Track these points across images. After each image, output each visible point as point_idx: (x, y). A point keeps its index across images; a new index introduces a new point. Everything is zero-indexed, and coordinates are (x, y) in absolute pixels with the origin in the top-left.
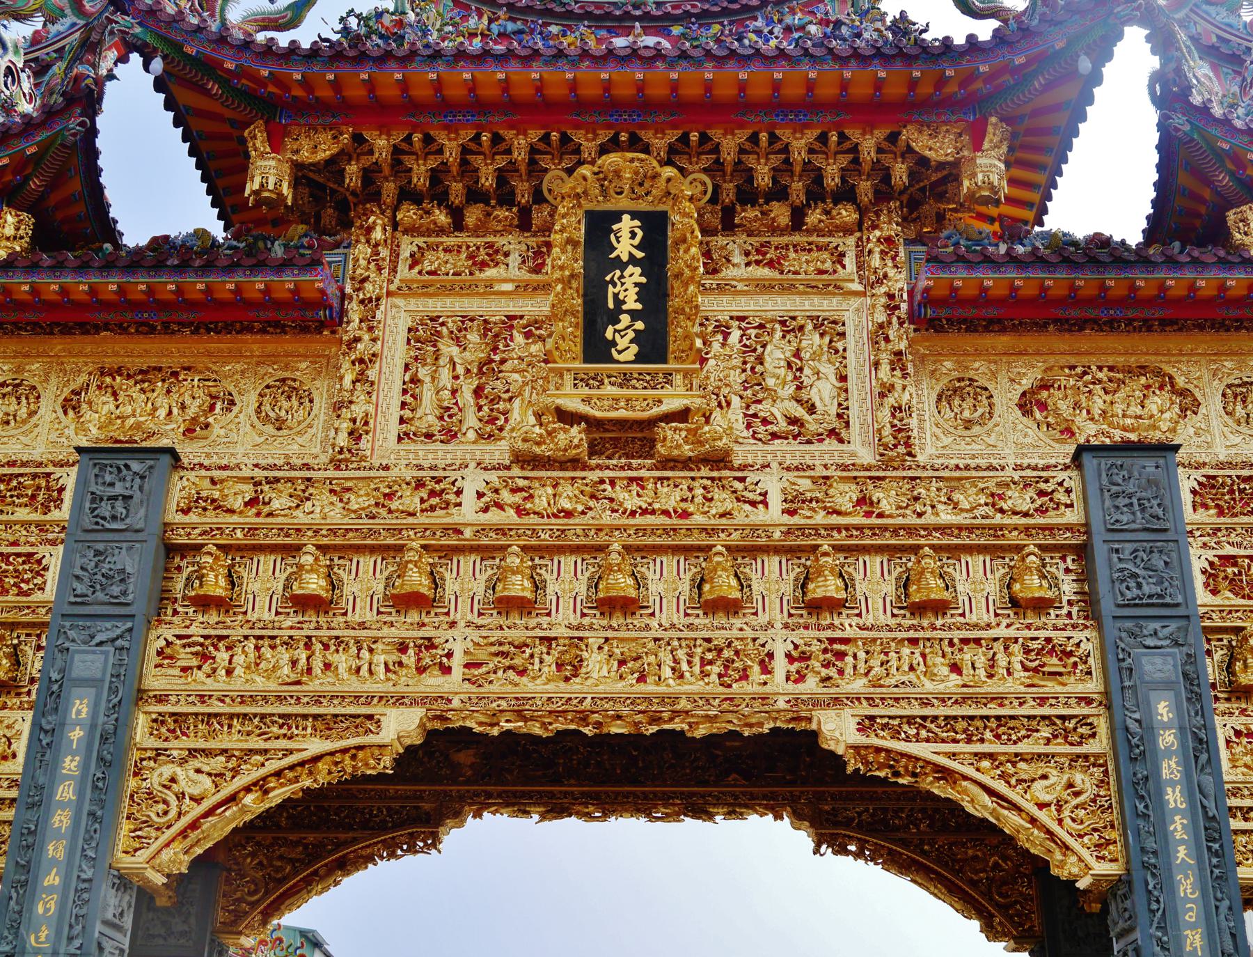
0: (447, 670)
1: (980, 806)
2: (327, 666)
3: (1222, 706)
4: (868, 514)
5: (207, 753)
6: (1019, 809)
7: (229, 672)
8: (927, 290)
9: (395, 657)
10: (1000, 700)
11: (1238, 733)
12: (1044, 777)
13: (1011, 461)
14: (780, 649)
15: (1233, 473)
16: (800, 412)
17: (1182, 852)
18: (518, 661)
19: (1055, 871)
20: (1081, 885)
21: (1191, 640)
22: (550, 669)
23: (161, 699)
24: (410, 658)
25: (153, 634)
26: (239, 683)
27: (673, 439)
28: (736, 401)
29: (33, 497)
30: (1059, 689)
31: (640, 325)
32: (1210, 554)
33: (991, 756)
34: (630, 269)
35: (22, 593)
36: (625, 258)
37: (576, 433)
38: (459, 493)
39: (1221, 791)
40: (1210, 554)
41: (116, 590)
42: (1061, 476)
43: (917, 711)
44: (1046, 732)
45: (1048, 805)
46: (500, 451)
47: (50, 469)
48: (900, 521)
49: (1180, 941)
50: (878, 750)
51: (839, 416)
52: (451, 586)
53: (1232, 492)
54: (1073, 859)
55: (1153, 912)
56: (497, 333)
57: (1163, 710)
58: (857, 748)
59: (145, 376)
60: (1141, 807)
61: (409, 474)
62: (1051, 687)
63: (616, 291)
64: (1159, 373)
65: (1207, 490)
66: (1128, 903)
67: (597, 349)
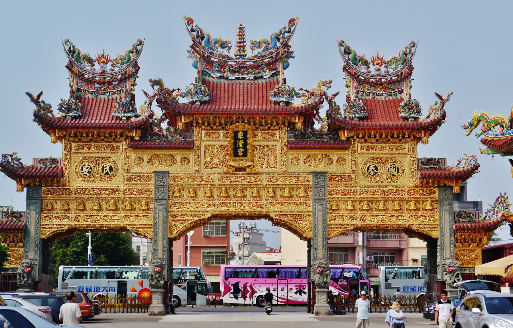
31: (243, 150)
67: (236, 154)
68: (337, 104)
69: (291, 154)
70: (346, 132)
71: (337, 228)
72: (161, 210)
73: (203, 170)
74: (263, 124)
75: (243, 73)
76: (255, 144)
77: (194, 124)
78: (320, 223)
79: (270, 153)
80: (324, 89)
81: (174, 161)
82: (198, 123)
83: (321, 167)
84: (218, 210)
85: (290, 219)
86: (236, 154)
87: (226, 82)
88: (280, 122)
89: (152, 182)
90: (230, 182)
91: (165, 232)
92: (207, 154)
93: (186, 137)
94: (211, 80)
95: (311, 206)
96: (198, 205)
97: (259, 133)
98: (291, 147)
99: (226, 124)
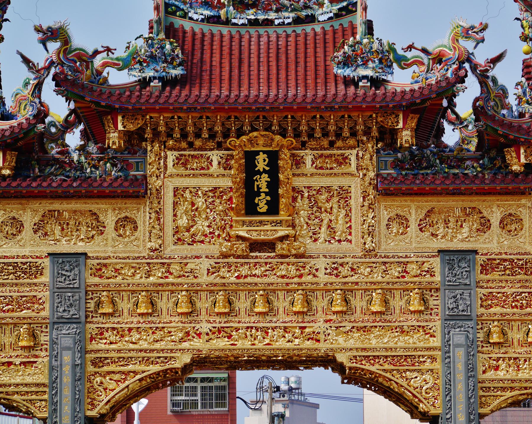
31: (268, 198)
34: (264, 175)
36: (261, 170)
63: (258, 184)
67: (251, 209)
68: (500, 81)
69: (386, 210)
70: (522, 151)
71: (503, 389)
72: (68, 349)
73: (171, 249)
74: (318, 134)
75: (266, 10)
76: (299, 182)
77: (148, 135)
78: (460, 376)
79: (335, 206)
80: (468, 45)
81: (99, 228)
82: (156, 134)
83: (461, 239)
84: (208, 346)
85: (386, 366)
86: (251, 209)
87: (225, 30)
88: (360, 128)
89: (45, 279)
90: (238, 277)
91: (77, 401)
92: (181, 210)
93: (126, 167)
94: (187, 25)
95: (438, 334)
96: (158, 335)
97: (308, 156)
98: (386, 189)
99: (226, 135)
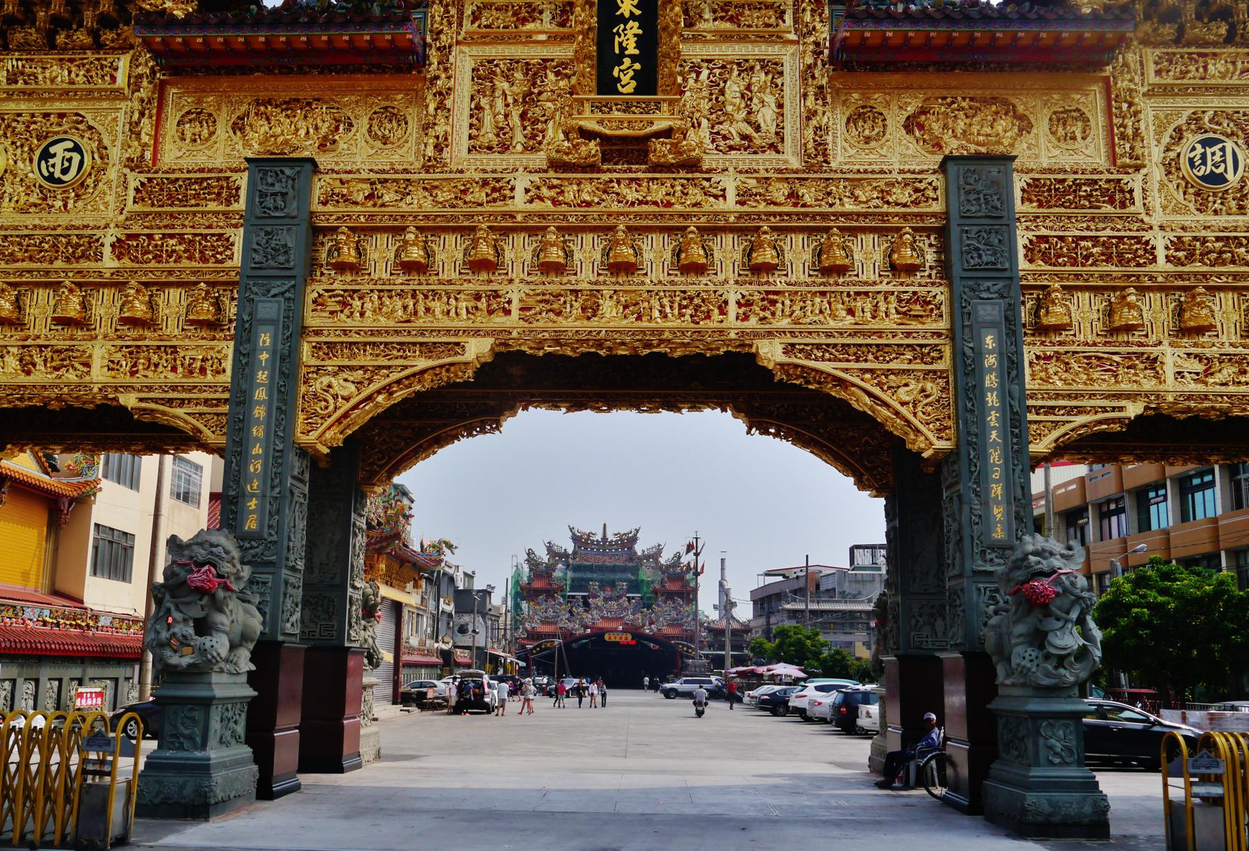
0: (508, 312)
1: (862, 403)
2: (428, 310)
3: (1029, 339)
4: (795, 205)
5: (352, 368)
6: (887, 406)
7: (362, 314)
8: (845, 39)
9: (472, 304)
10: (879, 333)
11: (1038, 357)
12: (906, 385)
13: (897, 167)
14: (732, 298)
15: (1052, 176)
16: (749, 130)
17: (994, 435)
18: (555, 306)
19: (909, 446)
20: (925, 455)
21: (1012, 294)
22: (577, 311)
23: (318, 333)
24: (483, 304)
25: (309, 289)
26: (369, 321)
27: (661, 150)
28: (704, 122)
29: (219, 194)
30: (920, 326)
31: (637, 66)
32: (1030, 235)
33: (872, 371)
34: (631, 23)
35: (218, 261)
36: (627, 15)
37: (593, 146)
38: (512, 189)
39: (1023, 396)
40: (1030, 235)
41: (282, 259)
42: (931, 178)
43: (824, 340)
44: (909, 356)
45: (908, 403)
46: (539, 159)
47: (228, 174)
48: (817, 209)
49: (988, 490)
50: (796, 366)
51: (777, 133)
52: (509, 255)
53: (1049, 190)
54: (922, 438)
55: (972, 473)
56: (535, 72)
57: (989, 341)
58: (782, 365)
59: (289, 105)
60: (969, 405)
61: (477, 176)
62: (915, 325)
64: (1005, 103)
65: (1034, 190)
66: (956, 467)
71: (1070, 411)
